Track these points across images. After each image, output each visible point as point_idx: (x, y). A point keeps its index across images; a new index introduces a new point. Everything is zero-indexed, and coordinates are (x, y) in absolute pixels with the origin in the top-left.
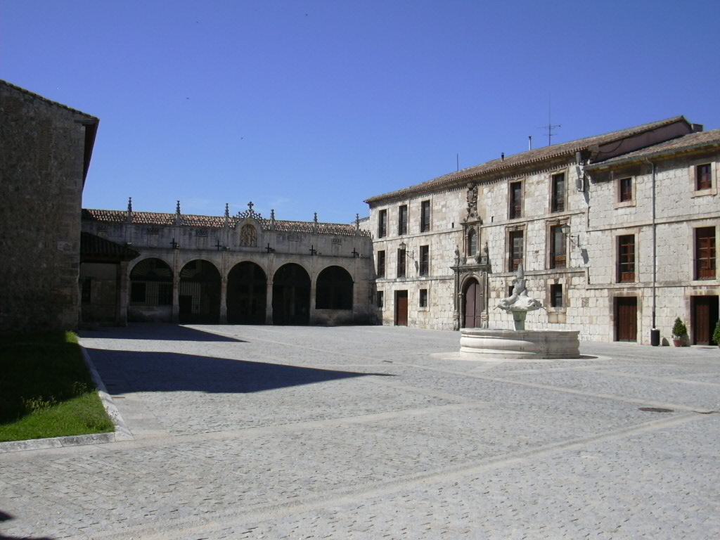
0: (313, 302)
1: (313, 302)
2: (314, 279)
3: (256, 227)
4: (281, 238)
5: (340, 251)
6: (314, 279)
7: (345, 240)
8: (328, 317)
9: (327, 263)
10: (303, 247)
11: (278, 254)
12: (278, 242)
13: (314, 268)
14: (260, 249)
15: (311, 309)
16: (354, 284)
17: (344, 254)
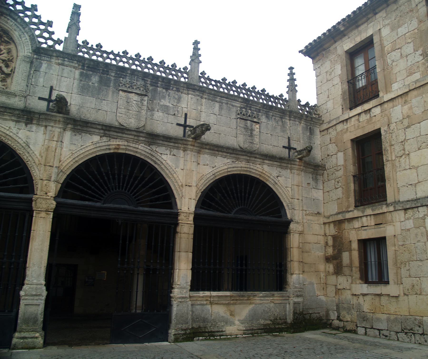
0: (183, 270)
1: (183, 270)
2: (187, 203)
3: (16, 34)
4: (95, 79)
5: (257, 140)
6: (187, 203)
7: (267, 117)
8: (227, 315)
9: (222, 166)
10: (158, 115)
11: (81, 126)
12: (84, 90)
13: (188, 177)
14: (17, 102)
15: (176, 292)
16: (292, 226)
17: (266, 148)
